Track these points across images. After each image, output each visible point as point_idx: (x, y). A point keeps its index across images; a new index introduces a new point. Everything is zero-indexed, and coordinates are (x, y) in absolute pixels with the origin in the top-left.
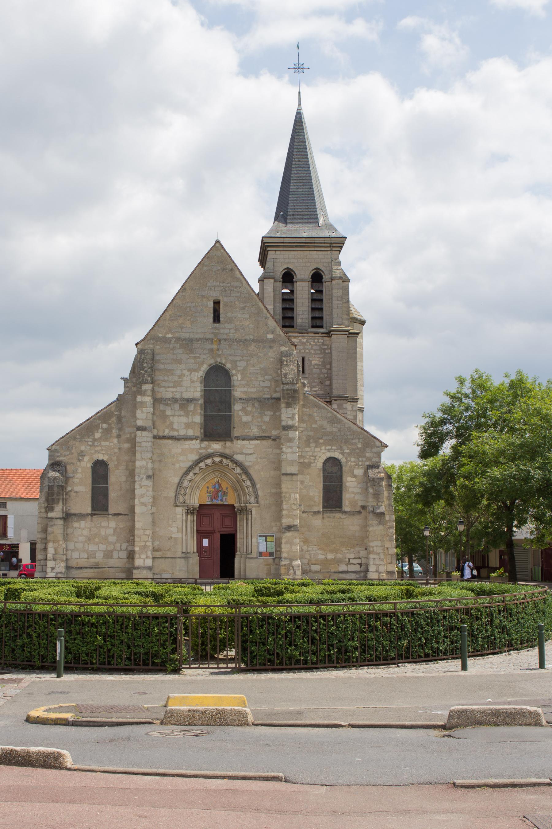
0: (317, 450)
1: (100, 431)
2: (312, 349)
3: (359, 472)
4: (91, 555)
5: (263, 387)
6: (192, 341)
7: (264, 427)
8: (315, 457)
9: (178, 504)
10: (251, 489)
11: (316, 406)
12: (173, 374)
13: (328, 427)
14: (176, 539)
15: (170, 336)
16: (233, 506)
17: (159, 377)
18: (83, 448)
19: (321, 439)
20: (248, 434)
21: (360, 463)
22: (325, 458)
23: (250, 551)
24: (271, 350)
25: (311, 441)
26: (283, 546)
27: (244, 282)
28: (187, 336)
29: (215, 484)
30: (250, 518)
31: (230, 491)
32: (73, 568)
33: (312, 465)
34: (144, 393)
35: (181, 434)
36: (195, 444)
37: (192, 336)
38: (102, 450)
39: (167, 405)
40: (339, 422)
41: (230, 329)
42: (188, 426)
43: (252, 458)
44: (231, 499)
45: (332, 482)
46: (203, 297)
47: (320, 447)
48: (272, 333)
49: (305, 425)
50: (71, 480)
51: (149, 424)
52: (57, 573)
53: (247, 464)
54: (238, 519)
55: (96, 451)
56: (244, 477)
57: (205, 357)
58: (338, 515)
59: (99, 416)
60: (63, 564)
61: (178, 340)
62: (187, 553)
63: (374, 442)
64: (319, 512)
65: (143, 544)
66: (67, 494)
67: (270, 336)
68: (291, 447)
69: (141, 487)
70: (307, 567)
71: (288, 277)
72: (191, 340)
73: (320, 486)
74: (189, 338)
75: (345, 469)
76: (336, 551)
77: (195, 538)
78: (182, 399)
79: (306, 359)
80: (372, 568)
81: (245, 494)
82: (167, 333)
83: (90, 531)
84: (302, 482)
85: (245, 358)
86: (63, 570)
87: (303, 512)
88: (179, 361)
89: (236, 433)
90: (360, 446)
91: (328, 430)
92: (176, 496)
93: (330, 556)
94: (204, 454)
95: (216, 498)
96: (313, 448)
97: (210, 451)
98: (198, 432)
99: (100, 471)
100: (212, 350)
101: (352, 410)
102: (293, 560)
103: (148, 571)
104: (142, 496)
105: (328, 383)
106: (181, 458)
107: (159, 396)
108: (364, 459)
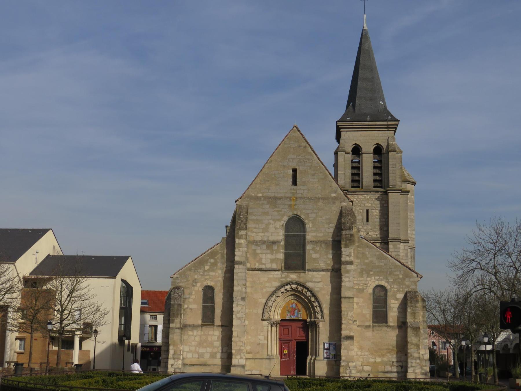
0: (369, 279)
1: (209, 264)
2: (374, 203)
3: (401, 296)
4: (201, 355)
5: (328, 233)
6: (276, 199)
7: (329, 262)
8: (367, 284)
10: (319, 309)
11: (367, 247)
12: (262, 223)
13: (377, 263)
14: (263, 345)
15: (260, 195)
17: (250, 225)
18: (196, 277)
19: (372, 271)
21: (401, 290)
22: (374, 286)
24: (334, 206)
25: (364, 272)
26: (342, 351)
27: (315, 156)
28: (272, 195)
32: (187, 365)
33: (365, 290)
34: (240, 237)
36: (278, 274)
37: (276, 195)
38: (210, 278)
39: (257, 245)
40: (386, 258)
41: (304, 190)
42: (272, 261)
43: (320, 285)
45: (380, 304)
46: (284, 166)
47: (371, 277)
48: (335, 193)
49: (359, 261)
50: (187, 301)
51: (242, 259)
52: (175, 369)
53: (316, 289)
55: (206, 279)
56: (313, 299)
57: (286, 210)
58: (385, 329)
59: (208, 253)
60: (180, 362)
61: (266, 198)
62: (272, 355)
63: (412, 274)
64: (370, 326)
65: (238, 348)
66: (184, 310)
67: (333, 195)
68: (349, 277)
69: (237, 305)
70: (360, 368)
71: (357, 150)
72: (276, 198)
73: (371, 307)
74: (274, 197)
75: (390, 294)
76: (383, 356)
77: (278, 344)
78: (268, 241)
79: (370, 211)
80: (410, 370)
81: (315, 312)
82: (258, 193)
83: (201, 338)
84: (357, 303)
85: (315, 211)
86: (180, 366)
87: (358, 326)
88: (267, 214)
89: (307, 267)
90: (401, 276)
91: (377, 264)
93: (379, 360)
94: (284, 282)
96: (365, 278)
97: (289, 280)
99: (208, 293)
100: (290, 205)
101: (405, 249)
102: (350, 362)
103: (242, 369)
104: (238, 312)
105: (385, 229)
106: (268, 285)
107: (251, 239)
108: (404, 287)
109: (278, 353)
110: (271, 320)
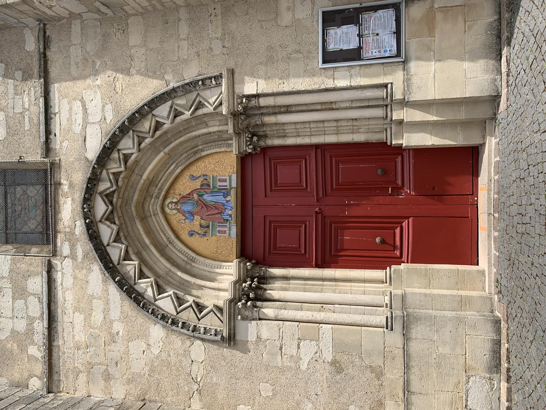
7: (19, 74)
9: (225, 334)
10: (181, 102)
16: (244, 160)
20: (35, 121)
23: (382, 93)
29: (183, 213)
30: (270, 101)
31: (198, 169)
35: (38, 315)
42: (20, 292)
44: (222, 167)
53: (110, 117)
54: (277, 142)
56: (146, 125)
89: (34, 156)
92: (203, 340)
95: (219, 209)
97: (80, 228)
98: (34, 261)
109: (378, 274)
110: (233, 302)
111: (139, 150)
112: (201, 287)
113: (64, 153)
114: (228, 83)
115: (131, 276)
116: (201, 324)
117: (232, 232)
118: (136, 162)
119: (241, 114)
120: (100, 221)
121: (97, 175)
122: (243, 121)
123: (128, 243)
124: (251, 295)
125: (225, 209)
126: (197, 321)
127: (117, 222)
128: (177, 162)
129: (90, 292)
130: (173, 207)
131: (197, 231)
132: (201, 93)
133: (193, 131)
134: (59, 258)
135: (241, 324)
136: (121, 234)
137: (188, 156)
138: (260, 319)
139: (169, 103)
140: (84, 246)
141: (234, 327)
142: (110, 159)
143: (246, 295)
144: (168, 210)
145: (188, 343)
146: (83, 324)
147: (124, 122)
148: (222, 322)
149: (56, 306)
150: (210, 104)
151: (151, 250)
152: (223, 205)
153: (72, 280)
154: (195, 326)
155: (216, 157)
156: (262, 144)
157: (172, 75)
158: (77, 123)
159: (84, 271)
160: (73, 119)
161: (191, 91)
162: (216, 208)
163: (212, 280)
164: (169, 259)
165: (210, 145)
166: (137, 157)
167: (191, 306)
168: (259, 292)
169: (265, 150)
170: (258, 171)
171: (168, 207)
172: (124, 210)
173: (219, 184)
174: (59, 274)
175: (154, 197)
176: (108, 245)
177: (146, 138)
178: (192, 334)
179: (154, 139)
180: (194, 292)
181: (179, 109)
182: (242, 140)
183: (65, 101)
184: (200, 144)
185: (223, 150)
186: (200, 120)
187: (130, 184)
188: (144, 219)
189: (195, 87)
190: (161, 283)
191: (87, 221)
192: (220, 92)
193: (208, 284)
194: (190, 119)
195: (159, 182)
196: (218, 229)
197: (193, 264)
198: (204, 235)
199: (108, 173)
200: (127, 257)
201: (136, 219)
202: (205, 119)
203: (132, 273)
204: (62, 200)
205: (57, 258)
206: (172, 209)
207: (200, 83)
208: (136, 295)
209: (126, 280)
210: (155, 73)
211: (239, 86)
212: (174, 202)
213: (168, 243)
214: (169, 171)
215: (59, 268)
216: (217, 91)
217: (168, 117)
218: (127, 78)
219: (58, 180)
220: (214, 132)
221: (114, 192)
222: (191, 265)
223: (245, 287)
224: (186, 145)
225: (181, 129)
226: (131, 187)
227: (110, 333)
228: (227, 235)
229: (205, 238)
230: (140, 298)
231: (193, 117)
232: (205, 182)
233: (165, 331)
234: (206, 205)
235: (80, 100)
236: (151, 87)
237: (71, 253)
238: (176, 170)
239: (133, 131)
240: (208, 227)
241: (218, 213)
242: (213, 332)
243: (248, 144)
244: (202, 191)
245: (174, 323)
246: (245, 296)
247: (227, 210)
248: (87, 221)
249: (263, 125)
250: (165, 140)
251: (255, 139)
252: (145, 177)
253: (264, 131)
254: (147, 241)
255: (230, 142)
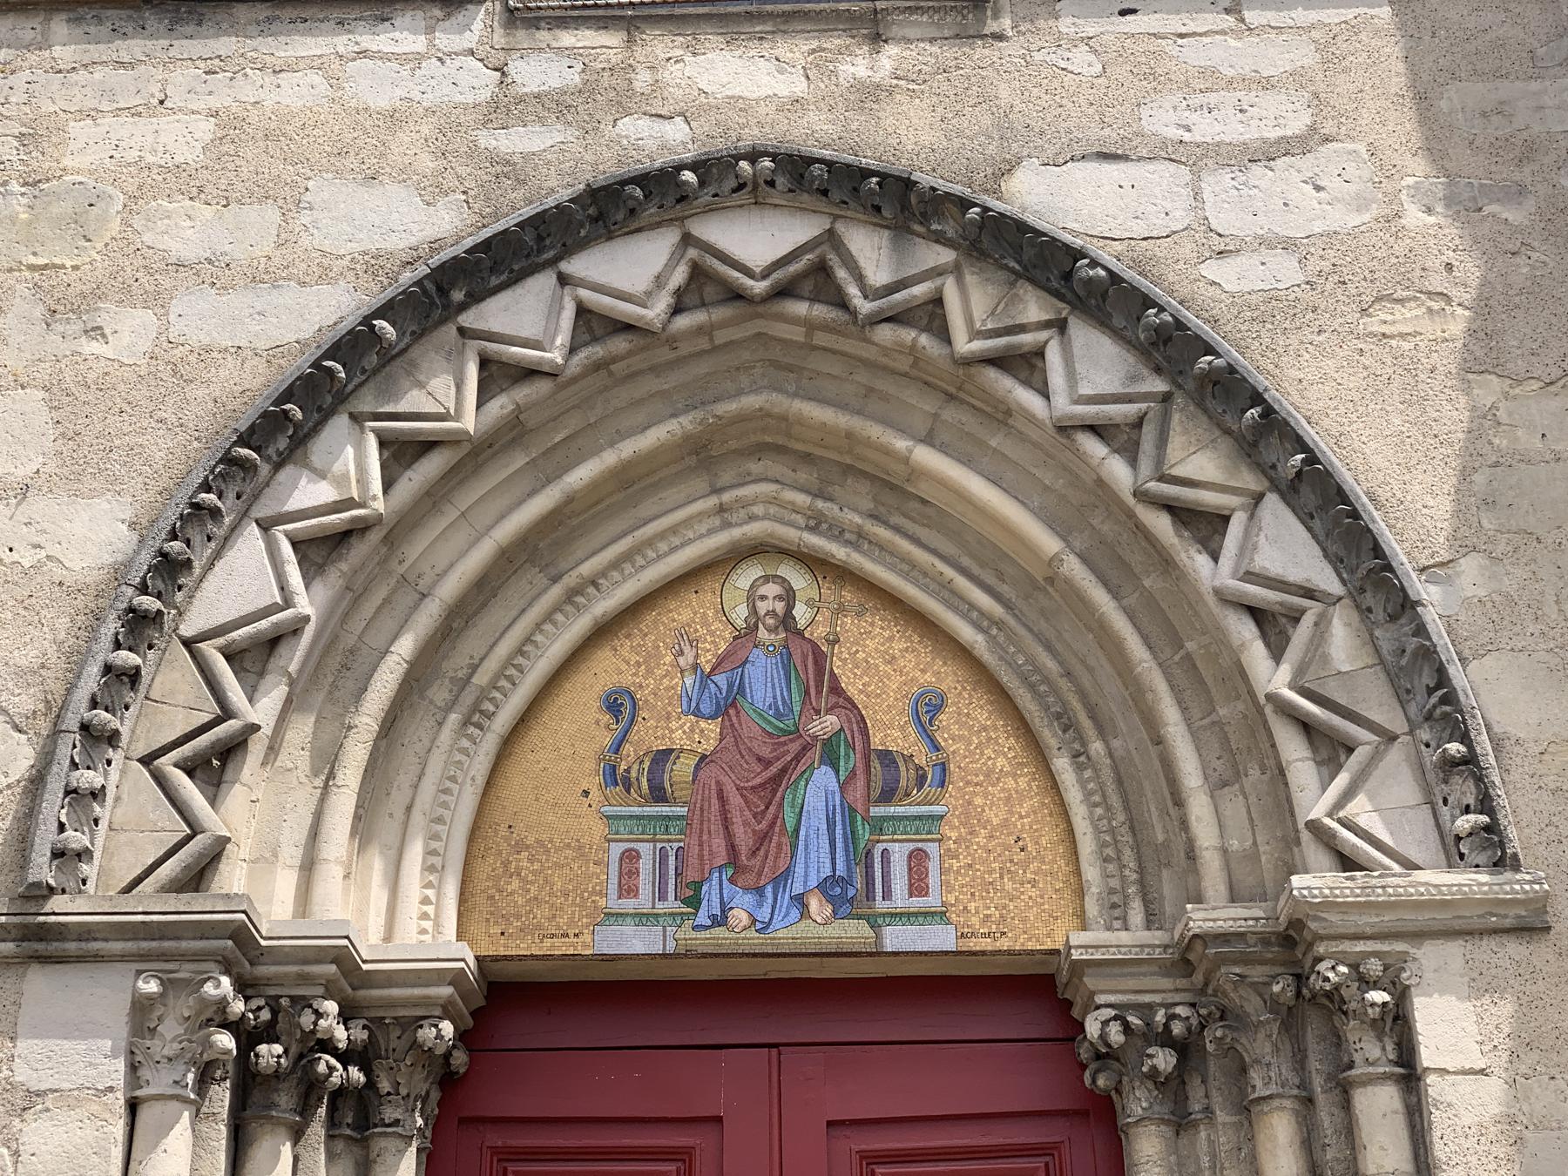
10: (1344, 644)
16: (1036, 992)
29: (733, 660)
31: (975, 736)
44: (995, 871)
53: (1235, 277)
56: (1201, 463)
92: (36, 782)
95: (758, 857)
110: (239, 946)
111: (1065, 429)
112: (327, 764)
113: (1038, 56)
114: (1467, 902)
115: (395, 396)
116: (123, 772)
117: (629, 929)
118: (1003, 415)
119: (1300, 979)
120: (687, 240)
121: (925, 219)
122: (1260, 988)
123: (574, 380)
124: (269, 1053)
125: (760, 891)
126: (142, 749)
127: (683, 322)
128: (1012, 622)
129: (321, 190)
130: (763, 607)
131: (633, 737)
132: (1396, 756)
133: (1184, 710)
134: (499, 38)
135: (107, 994)
136: (620, 344)
137: (1046, 680)
138: (133, 1107)
139: (1327, 579)
140: (555, 160)
141: (97, 958)
142: (1012, 284)
143: (273, 1021)
144: (746, 576)
145: (24, 702)
146: (150, 159)
147: (1210, 350)
148: (129, 889)
149: (253, 29)
150: (1341, 803)
151: (532, 493)
152: (782, 879)
153: (382, 102)
154: (113, 738)
155: (1049, 835)
156: (1138, 1102)
157: (1482, 593)
158: (1194, 117)
159: (427, 163)
160: (1212, 98)
161: (1403, 697)
162: (763, 838)
163: (363, 826)
164: (485, 588)
165: (1115, 800)
166: (1030, 418)
167: (226, 713)
168: (285, 1100)
169: (1102, 1118)
170: (982, 1079)
171: (767, 579)
172: (746, 355)
173: (899, 853)
174: (418, 43)
175: (820, 504)
176: (563, 280)
177: (1133, 462)
178: (71, 722)
179: (1131, 501)
180: (301, 730)
181: (1301, 635)
182: (1148, 982)
183: (1303, 55)
184: (1116, 743)
185: (1091, 873)
186: (1245, 743)
187: (884, 384)
188: (698, 457)
189: (1429, 717)
190: (359, 550)
191: (688, 176)
192: (1414, 855)
193: (344, 803)
194: (1251, 693)
195: (897, 529)
196: (645, 849)
197: (454, 718)
198: (613, 776)
199: (937, 272)
200: (497, 374)
201: (698, 414)
202: (1254, 772)
203: (414, 400)
204: (796, 49)
205: (499, 31)
206: (752, 598)
207: (1455, 748)
208: (297, 426)
209: (376, 371)
210: (1488, 503)
211: (1457, 963)
212: (790, 608)
213: (570, 580)
214: (962, 582)
215: (446, 40)
216: (1417, 838)
217: (1250, 576)
218: (1447, 360)
219: (895, 31)
220: (1184, 824)
221: (843, 304)
222: (449, 709)
223: (319, 1015)
224: (1105, 670)
225: (1190, 646)
226: (870, 391)
227: (98, 294)
228: (614, 903)
229: (593, 783)
230: (282, 443)
231: (1259, 713)
232: (906, 776)
233: (94, 577)
234: (776, 780)
235: (1313, 128)
236: (1408, 485)
237: (521, 100)
238: (965, 616)
239: (1166, 398)
240: (658, 794)
241: (732, 848)
242: (76, 839)
243: (1133, 1020)
244: (856, 759)
245: (139, 626)
246: (265, 1015)
247: (749, 899)
248: (688, 176)
249: (1247, 1109)
250: (1125, 557)
251: (1164, 1060)
252: (925, 456)
253: (1208, 1110)
254: (581, 475)
255: (1136, 915)
